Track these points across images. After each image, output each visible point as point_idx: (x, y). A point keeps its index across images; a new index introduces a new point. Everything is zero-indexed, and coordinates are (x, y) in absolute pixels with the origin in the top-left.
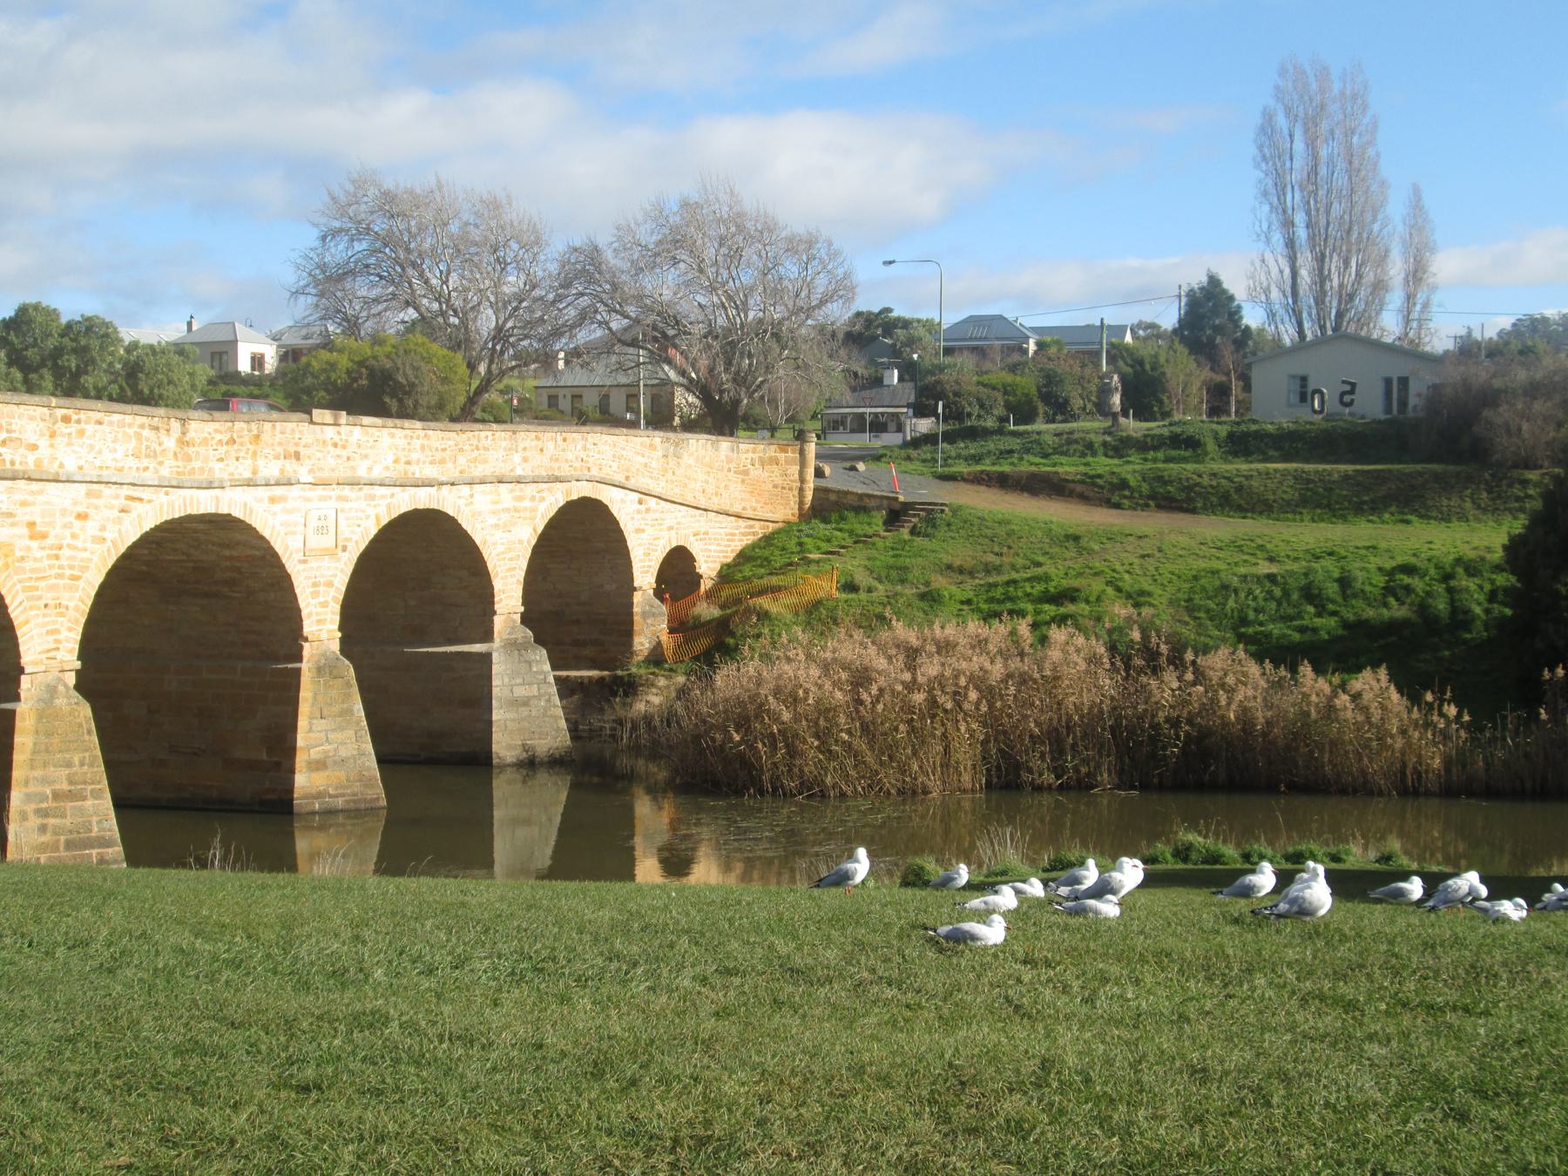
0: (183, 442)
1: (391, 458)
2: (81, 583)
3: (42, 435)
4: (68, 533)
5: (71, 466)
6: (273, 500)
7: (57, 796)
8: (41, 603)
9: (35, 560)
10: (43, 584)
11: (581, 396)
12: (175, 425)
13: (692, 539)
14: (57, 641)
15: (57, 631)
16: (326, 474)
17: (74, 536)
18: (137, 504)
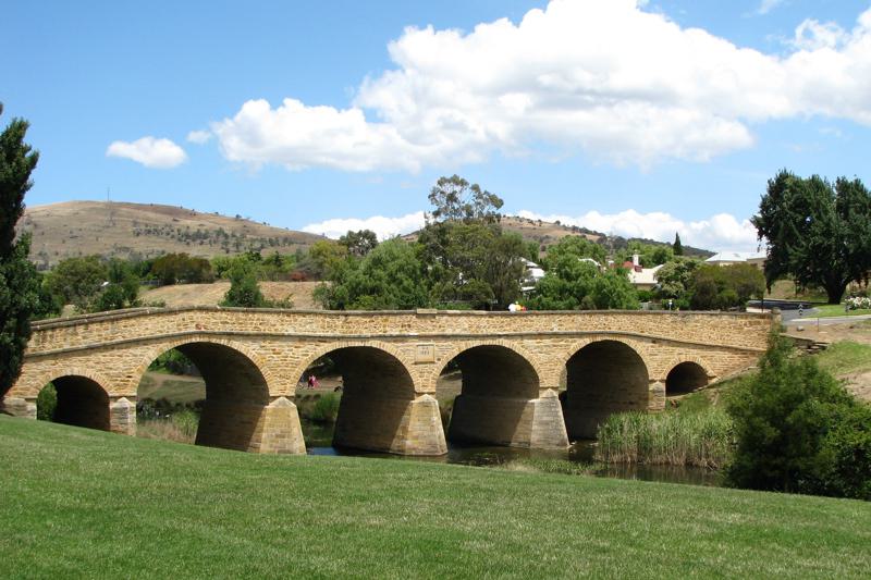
1: (467, 326)
5: (291, 332)
7: (277, 436)
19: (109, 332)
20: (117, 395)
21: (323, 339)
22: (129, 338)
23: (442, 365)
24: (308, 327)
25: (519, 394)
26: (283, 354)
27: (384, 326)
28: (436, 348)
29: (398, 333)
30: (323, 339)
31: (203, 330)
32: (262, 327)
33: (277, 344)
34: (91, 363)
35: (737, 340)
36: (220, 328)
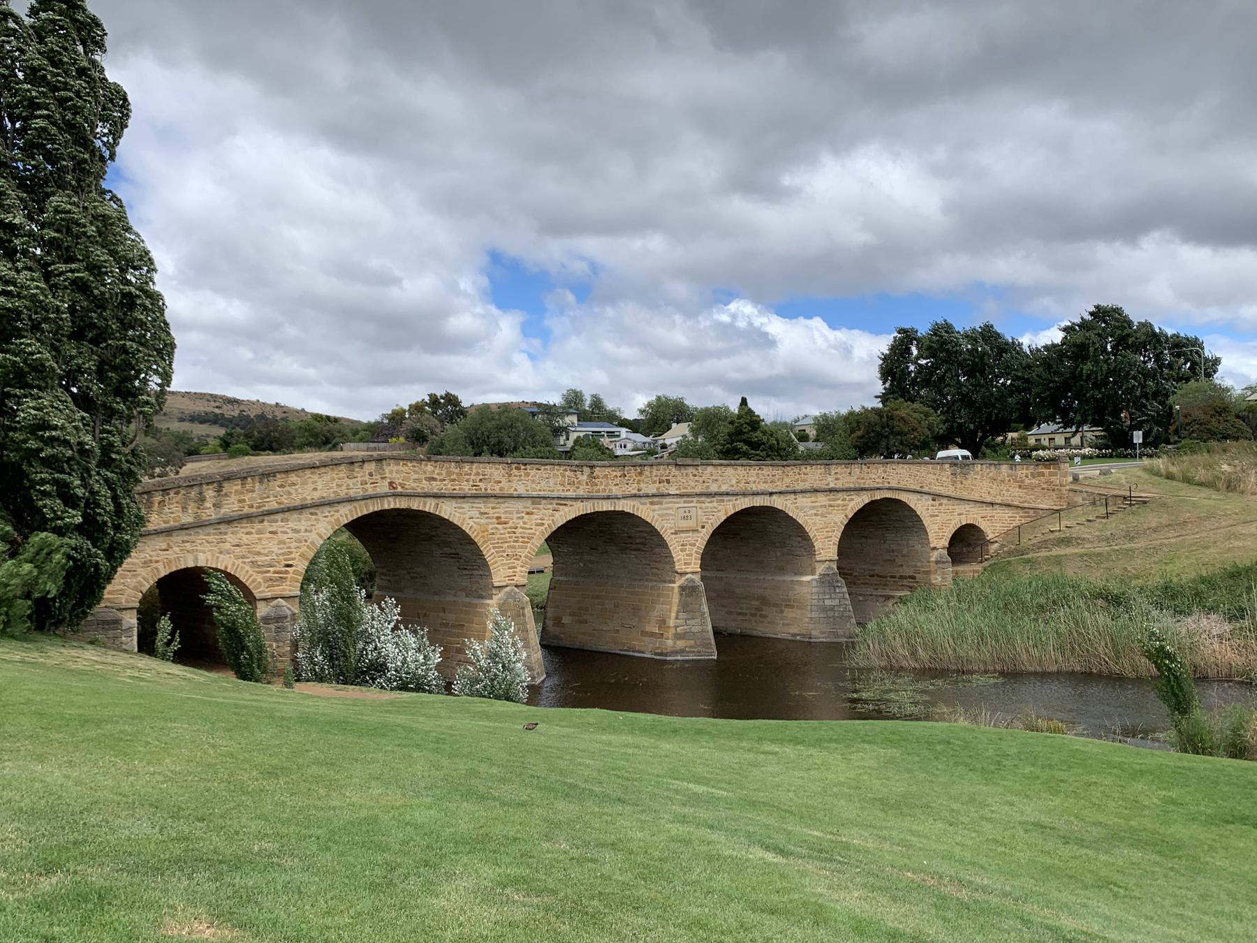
0: (591, 476)
1: (734, 482)
2: (529, 545)
3: (503, 476)
4: (521, 521)
5: (521, 490)
6: (652, 503)
8: (505, 555)
9: (501, 534)
10: (506, 545)
11: (1054, 439)
12: (587, 470)
13: (981, 520)
14: (514, 572)
15: (515, 567)
16: (689, 490)
17: (524, 523)
18: (561, 507)
19: (255, 495)
20: (269, 595)
21: (562, 500)
22: (286, 502)
23: (705, 534)
24: (543, 483)
25: (782, 570)
26: (510, 524)
27: (639, 482)
28: (700, 512)
29: (654, 491)
30: (562, 500)
31: (400, 489)
32: (482, 485)
33: (503, 509)
34: (227, 546)
35: (1015, 494)
36: (426, 486)
